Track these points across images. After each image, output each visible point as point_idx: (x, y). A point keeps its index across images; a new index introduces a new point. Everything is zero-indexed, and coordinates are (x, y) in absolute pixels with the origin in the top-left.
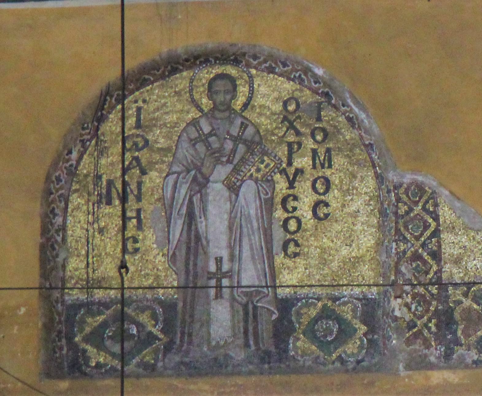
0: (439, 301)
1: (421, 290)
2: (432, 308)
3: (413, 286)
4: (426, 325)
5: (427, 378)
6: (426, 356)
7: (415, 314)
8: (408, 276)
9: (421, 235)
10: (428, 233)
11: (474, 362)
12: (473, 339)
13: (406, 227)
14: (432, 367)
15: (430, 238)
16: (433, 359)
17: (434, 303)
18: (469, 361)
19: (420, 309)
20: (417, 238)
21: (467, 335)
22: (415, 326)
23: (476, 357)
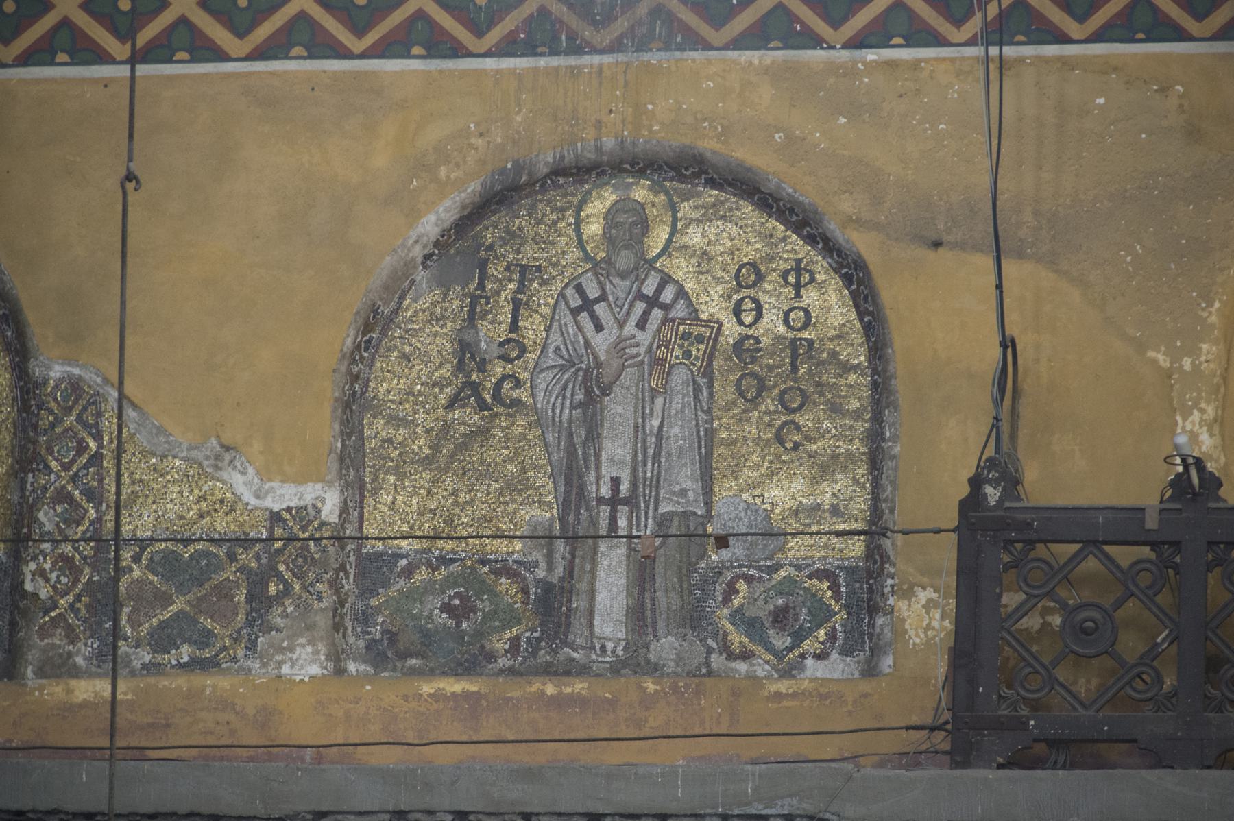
0: (94, 568)
1: (67, 548)
2: (84, 579)
3: (56, 542)
4: (72, 606)
5: (69, 691)
6: (70, 655)
7: (54, 587)
8: (49, 527)
9: (73, 461)
10: (84, 459)
11: (145, 666)
12: (144, 630)
13: (50, 451)
14: (75, 673)
15: (86, 467)
16: (79, 660)
17: (87, 570)
18: (137, 664)
19: (64, 580)
20: (66, 467)
21: (135, 625)
22: (55, 607)
23: (147, 658)
